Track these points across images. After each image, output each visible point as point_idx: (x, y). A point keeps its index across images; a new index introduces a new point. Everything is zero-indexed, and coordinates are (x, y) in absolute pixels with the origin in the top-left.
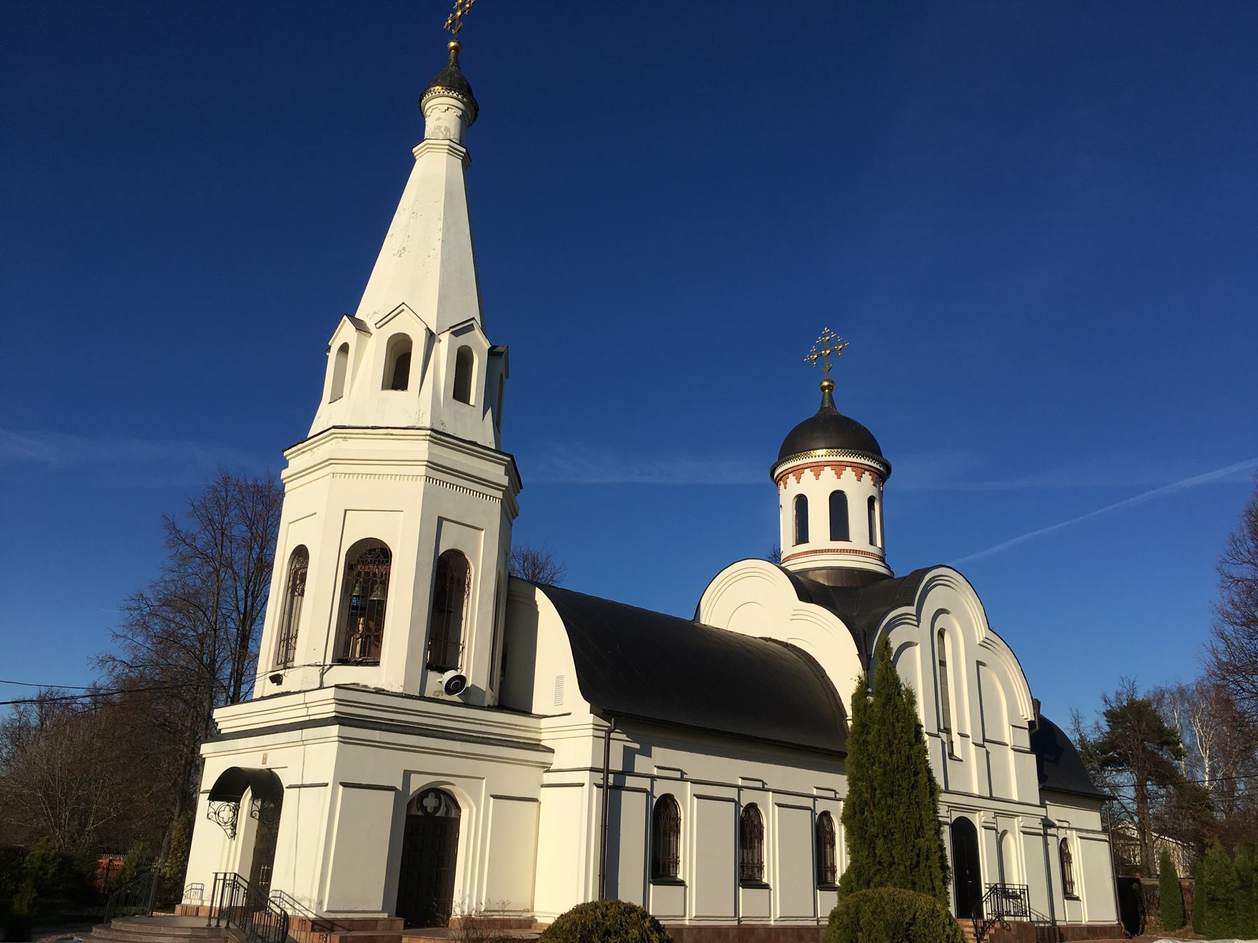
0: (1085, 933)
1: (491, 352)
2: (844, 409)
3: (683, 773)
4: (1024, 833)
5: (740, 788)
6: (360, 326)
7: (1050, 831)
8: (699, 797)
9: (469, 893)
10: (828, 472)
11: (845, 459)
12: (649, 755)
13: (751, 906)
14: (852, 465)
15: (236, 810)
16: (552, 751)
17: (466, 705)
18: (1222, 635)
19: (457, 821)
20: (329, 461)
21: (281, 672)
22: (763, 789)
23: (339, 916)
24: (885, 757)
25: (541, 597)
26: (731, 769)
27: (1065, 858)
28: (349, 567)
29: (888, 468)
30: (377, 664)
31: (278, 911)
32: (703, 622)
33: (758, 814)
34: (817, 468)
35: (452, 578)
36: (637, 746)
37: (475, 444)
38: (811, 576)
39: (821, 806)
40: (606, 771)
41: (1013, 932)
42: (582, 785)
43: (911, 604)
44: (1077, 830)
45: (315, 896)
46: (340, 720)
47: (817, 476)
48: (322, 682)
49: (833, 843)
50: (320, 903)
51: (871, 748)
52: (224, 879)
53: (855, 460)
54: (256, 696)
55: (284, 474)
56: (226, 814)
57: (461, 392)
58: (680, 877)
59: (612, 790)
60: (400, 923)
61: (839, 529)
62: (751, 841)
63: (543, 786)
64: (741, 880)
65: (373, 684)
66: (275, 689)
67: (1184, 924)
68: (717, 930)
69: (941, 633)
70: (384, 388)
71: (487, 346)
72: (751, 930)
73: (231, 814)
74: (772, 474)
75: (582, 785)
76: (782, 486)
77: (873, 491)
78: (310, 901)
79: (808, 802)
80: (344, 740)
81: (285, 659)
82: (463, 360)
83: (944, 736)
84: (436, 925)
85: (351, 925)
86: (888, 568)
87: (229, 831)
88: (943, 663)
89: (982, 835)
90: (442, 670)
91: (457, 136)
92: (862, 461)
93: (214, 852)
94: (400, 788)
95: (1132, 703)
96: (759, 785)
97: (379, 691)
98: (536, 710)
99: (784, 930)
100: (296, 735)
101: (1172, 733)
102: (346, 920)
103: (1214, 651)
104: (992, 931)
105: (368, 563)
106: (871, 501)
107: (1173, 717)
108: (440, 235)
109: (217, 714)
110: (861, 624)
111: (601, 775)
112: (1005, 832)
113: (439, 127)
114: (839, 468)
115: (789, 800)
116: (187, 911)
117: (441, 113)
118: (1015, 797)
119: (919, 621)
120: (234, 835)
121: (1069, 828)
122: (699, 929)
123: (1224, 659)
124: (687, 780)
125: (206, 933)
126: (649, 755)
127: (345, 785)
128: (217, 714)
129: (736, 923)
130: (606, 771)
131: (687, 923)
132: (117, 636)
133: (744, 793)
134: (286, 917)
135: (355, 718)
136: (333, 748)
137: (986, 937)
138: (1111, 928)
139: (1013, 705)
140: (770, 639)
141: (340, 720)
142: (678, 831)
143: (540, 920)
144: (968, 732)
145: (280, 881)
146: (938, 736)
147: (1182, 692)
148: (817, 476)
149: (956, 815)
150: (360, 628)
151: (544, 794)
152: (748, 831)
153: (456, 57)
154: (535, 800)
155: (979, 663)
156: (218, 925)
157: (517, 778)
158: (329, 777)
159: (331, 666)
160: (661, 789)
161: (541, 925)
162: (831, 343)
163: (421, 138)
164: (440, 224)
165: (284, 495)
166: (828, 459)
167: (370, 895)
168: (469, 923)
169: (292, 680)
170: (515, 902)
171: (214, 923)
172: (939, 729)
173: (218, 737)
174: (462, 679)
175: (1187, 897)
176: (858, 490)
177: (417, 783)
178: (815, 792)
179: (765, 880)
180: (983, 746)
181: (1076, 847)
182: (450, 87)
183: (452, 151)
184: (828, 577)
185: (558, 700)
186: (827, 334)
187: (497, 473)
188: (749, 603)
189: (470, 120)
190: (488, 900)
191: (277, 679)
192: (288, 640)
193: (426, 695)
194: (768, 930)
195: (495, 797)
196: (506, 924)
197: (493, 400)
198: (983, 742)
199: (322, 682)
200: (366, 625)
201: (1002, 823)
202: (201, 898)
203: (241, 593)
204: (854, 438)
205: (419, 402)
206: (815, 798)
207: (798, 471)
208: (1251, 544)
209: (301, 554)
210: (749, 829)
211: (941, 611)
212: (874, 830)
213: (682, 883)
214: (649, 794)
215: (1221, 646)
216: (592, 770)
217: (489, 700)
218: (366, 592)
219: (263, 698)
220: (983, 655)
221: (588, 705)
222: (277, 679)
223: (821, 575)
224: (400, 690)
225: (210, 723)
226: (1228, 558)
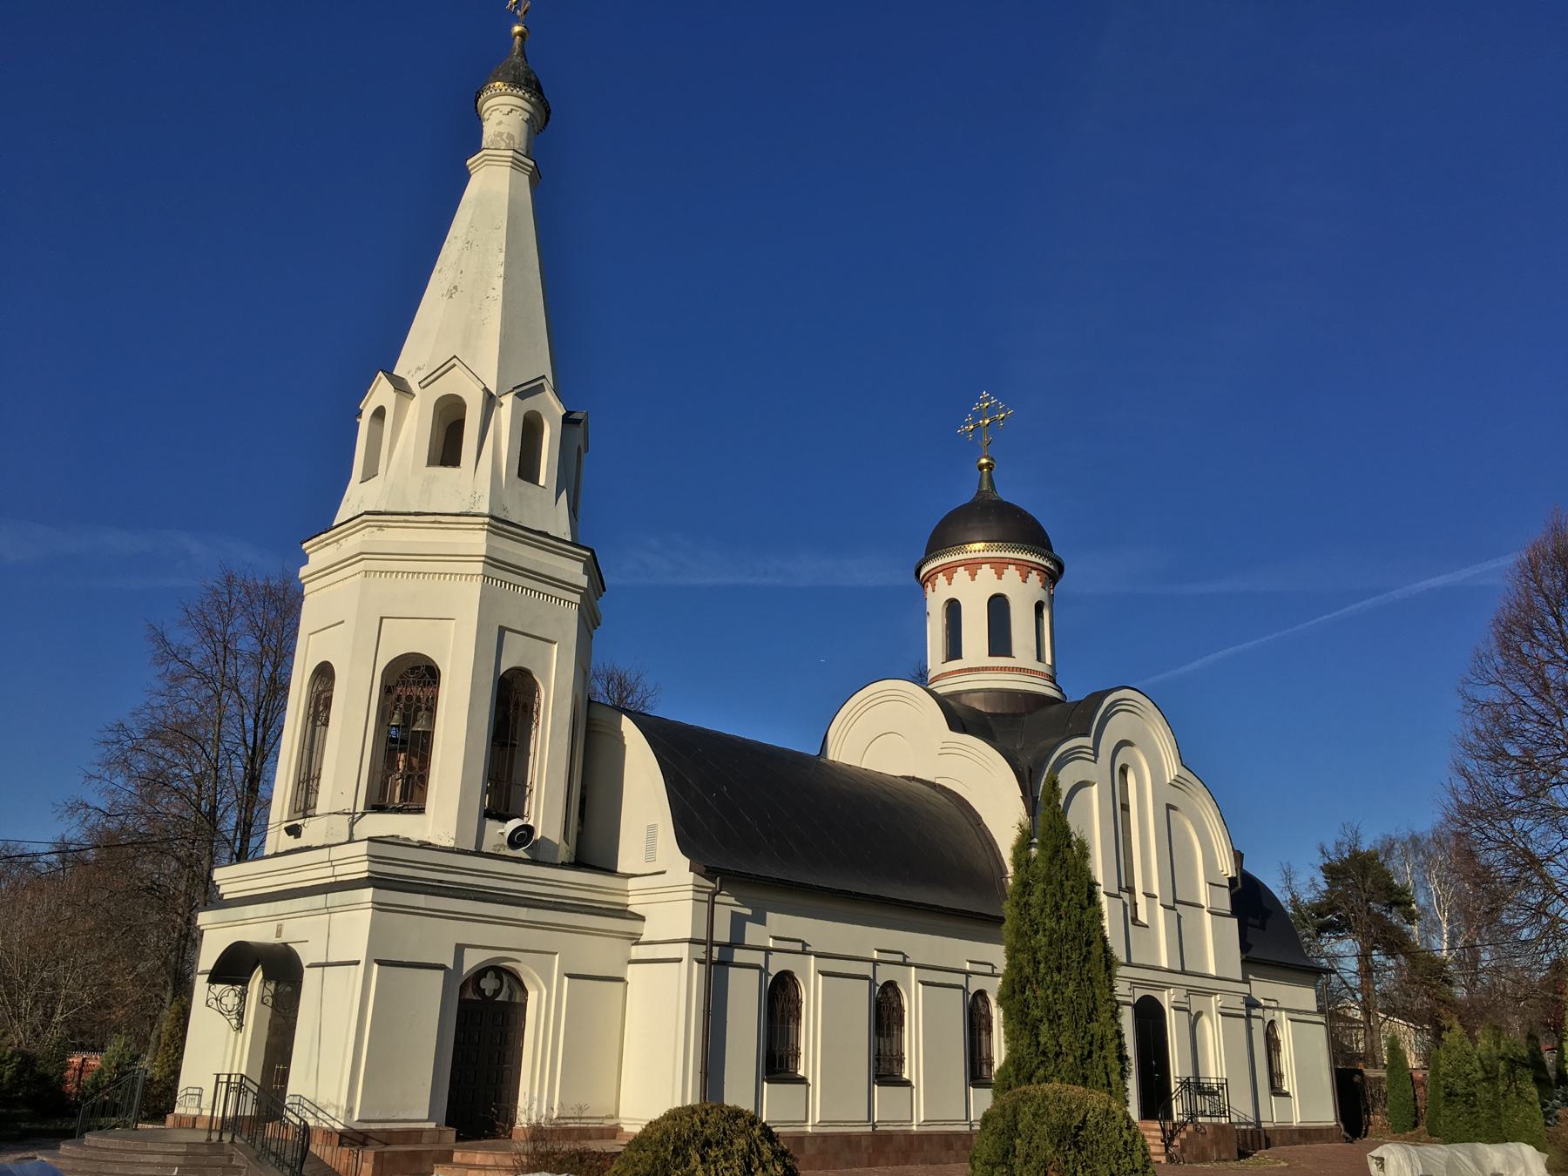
0: (1296, 1137)
1: (567, 420)
2: (1005, 494)
3: (805, 945)
4: (1223, 1015)
5: (876, 962)
6: (401, 386)
7: (1254, 1012)
8: (824, 974)
9: (537, 1096)
10: (986, 571)
11: (1007, 555)
12: (763, 923)
13: (889, 1108)
14: (1018, 564)
15: (243, 996)
16: (642, 919)
17: (534, 862)
18: (1463, 772)
19: (524, 1006)
20: (361, 556)
21: (299, 822)
22: (904, 964)
23: (373, 1126)
24: (1051, 924)
26: (864, 939)
27: (1272, 1045)
28: (387, 690)
30: (421, 811)
31: (297, 1121)
32: (830, 757)
33: (898, 994)
34: (973, 566)
35: (517, 704)
36: (748, 912)
37: (545, 535)
38: (965, 700)
39: (975, 984)
40: (710, 943)
41: (1209, 1136)
42: (680, 960)
43: (1087, 735)
44: (1288, 1010)
45: (343, 1102)
46: (374, 881)
47: (973, 576)
48: (351, 834)
50: (350, 1111)
51: (1034, 912)
52: (228, 1082)
53: (1020, 556)
54: (268, 851)
55: (304, 571)
56: (231, 1000)
57: (527, 468)
58: (801, 1073)
59: (716, 963)
60: (451, 1133)
61: (1000, 642)
62: (889, 1028)
64: (877, 1076)
65: (416, 836)
66: (291, 842)
67: (1416, 1125)
68: (847, 1139)
69: (1124, 770)
70: (430, 463)
71: (561, 411)
72: (889, 1137)
73: (237, 1000)
75: (680, 960)
76: (929, 589)
77: (1042, 595)
78: (337, 1108)
79: (959, 979)
80: (379, 907)
81: (305, 804)
82: (530, 430)
83: (1125, 896)
84: (495, 1136)
85: (389, 1137)
86: (1060, 691)
87: (234, 1022)
88: (1125, 807)
89: (1171, 1017)
90: (504, 819)
91: (523, 146)
92: (1028, 557)
93: (215, 1049)
94: (450, 966)
95: (1355, 854)
96: (899, 958)
97: (424, 845)
99: (928, 1137)
100: (319, 900)
101: (1403, 891)
102: (384, 1131)
103: (1454, 792)
104: (1183, 1135)
105: (411, 682)
106: (1039, 607)
107: (1404, 873)
108: (501, 270)
110: (1026, 760)
112: (1199, 1014)
113: (500, 134)
114: (999, 566)
115: (935, 977)
116: (181, 1122)
117: (503, 114)
118: (1212, 971)
119: (1096, 755)
120: (240, 1026)
121: (1280, 1009)
122: (825, 1137)
123: (1466, 801)
124: (810, 953)
125: (205, 1150)
126: (761, 921)
127: (381, 963)
128: (219, 874)
129: (870, 1129)
130: (710, 943)
131: (809, 1129)
132: (90, 777)
133: (881, 968)
134: (306, 1130)
135: (395, 880)
136: (366, 916)
137: (1176, 1142)
138: (1329, 1129)
139: (1211, 857)
140: (914, 779)
141: (374, 881)
142: (799, 1017)
143: (627, 1129)
144: (1156, 892)
145: (297, 1084)
146: (1118, 897)
147: (1415, 840)
148: (973, 576)
149: (1139, 993)
150: (400, 767)
151: (632, 972)
152: (885, 1015)
153: (522, 46)
154: (621, 980)
155: (1169, 807)
156: (220, 1139)
157: (597, 953)
158: (361, 955)
159: (364, 814)
160: (777, 964)
161: (628, 1134)
162: (991, 411)
163: (477, 148)
164: (502, 257)
165: (303, 598)
166: (986, 554)
167: (416, 1101)
168: (538, 1133)
169: (313, 831)
170: (596, 1108)
171: (215, 1137)
172: (1120, 888)
173: (219, 903)
174: (530, 830)
175: (1420, 1091)
176: (1023, 592)
177: (472, 960)
178: (968, 966)
179: (906, 1076)
180: (1173, 909)
181: (1285, 1033)
182: (515, 82)
183: (516, 164)
184: (986, 701)
186: (986, 400)
187: (574, 571)
188: (887, 734)
189: (541, 123)
190: (561, 1105)
191: (294, 831)
192: (308, 781)
193: (485, 849)
194: (909, 1137)
195: (570, 976)
196: (584, 1134)
197: (569, 480)
198: (1177, 904)
199: (351, 834)
200: (408, 762)
201: (1196, 1003)
202: (199, 1106)
203: (249, 723)
204: (1021, 530)
205: (473, 482)
206: (968, 974)
207: (949, 570)
208: (1499, 660)
209: (324, 673)
210: (886, 1013)
211: (1124, 743)
212: (1037, 1013)
213: (803, 1081)
214: (763, 971)
215: (1462, 784)
216: (692, 941)
217: (564, 854)
218: (408, 720)
219: (276, 855)
220: (1174, 797)
221: (685, 862)
222: (294, 831)
224: (451, 844)
225: (209, 885)
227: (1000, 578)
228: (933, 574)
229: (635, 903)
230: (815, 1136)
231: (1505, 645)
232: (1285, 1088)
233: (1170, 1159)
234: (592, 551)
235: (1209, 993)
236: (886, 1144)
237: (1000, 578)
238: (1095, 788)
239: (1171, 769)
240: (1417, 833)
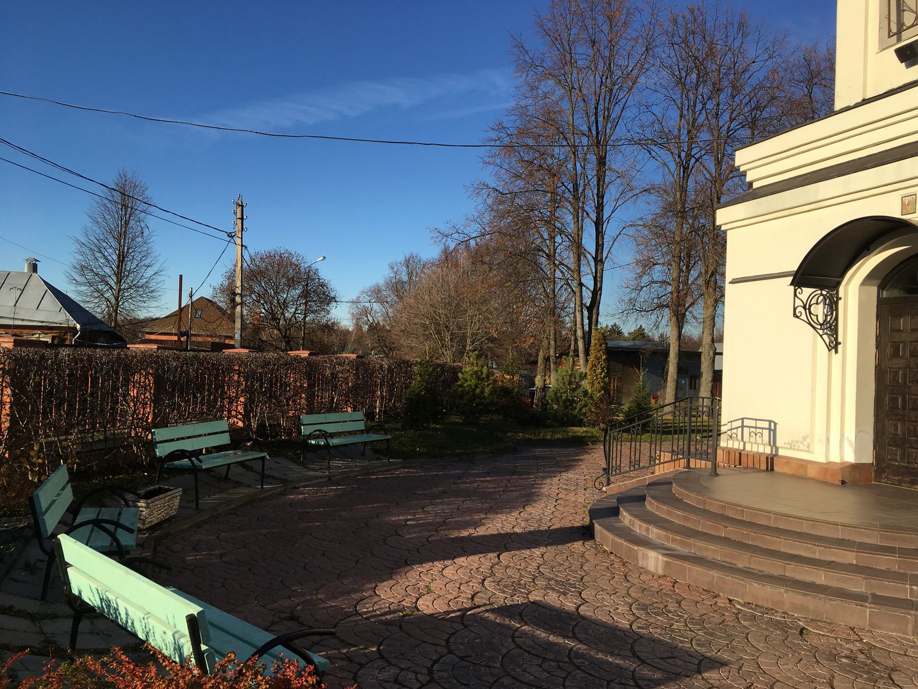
15: (833, 304)
56: (819, 311)
109: (743, 157)
116: (739, 458)
120: (834, 346)
128: (743, 157)
202: (773, 442)
219: (865, 102)
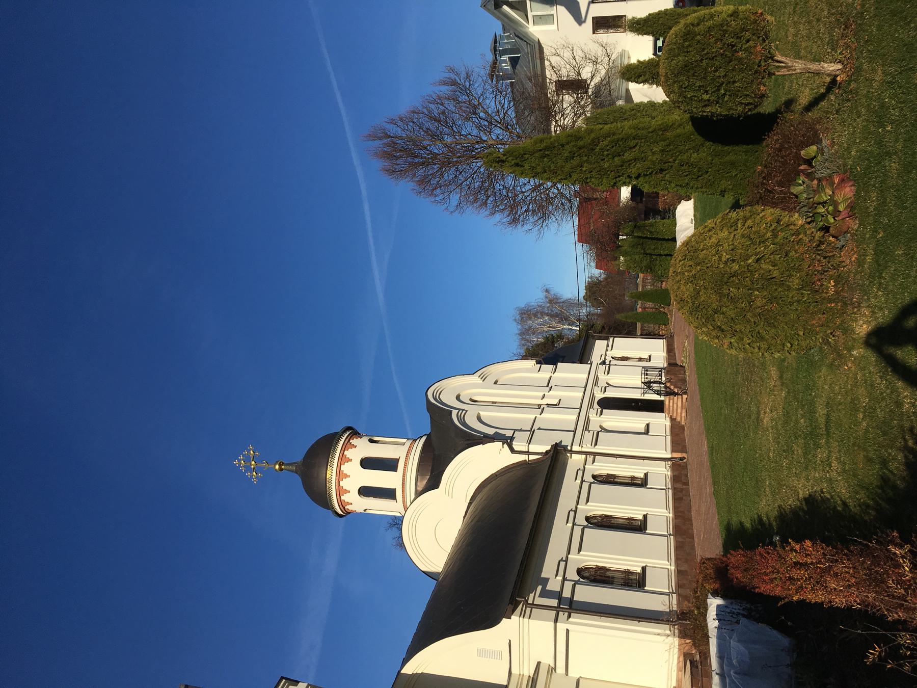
2: (299, 457)
5: (574, 524)
8: (580, 550)
10: (345, 468)
12: (546, 580)
14: (344, 449)
16: (539, 663)
22: (576, 511)
25: (410, 669)
29: (349, 428)
33: (595, 517)
34: (340, 476)
38: (420, 489)
42: (568, 631)
43: (451, 412)
44: (607, 350)
47: (347, 476)
49: (614, 476)
59: (571, 606)
61: (389, 465)
62: (609, 577)
63: (567, 674)
68: (677, 548)
69: (471, 400)
74: (341, 516)
75: (568, 631)
79: (585, 486)
89: (611, 394)
96: (572, 514)
98: (505, 683)
101: (547, 339)
104: (672, 387)
106: (371, 441)
111: (561, 613)
114: (343, 459)
119: (463, 410)
121: (606, 355)
122: (677, 559)
124: (567, 558)
126: (546, 580)
130: (557, 609)
131: (673, 568)
137: (676, 390)
144: (541, 394)
147: (520, 334)
148: (347, 476)
149: (596, 405)
151: (574, 673)
155: (496, 383)
160: (572, 575)
162: (247, 459)
166: (335, 469)
176: (362, 448)
178: (579, 481)
179: (641, 517)
185: (496, 655)
188: (434, 529)
201: (602, 383)
204: (323, 449)
206: (582, 481)
207: (340, 491)
210: (605, 523)
211: (458, 398)
215: (498, 217)
216: (556, 621)
221: (504, 620)
223: (422, 480)
226: (445, 206)
227: (349, 460)
228: (342, 504)
229: (529, 671)
230: (677, 565)
231: (432, 193)
232: (647, 357)
233: (685, 393)
234: (282, 678)
235: (597, 380)
236: (682, 529)
237: (349, 460)
238: (482, 413)
239: (475, 379)
240: (517, 332)
